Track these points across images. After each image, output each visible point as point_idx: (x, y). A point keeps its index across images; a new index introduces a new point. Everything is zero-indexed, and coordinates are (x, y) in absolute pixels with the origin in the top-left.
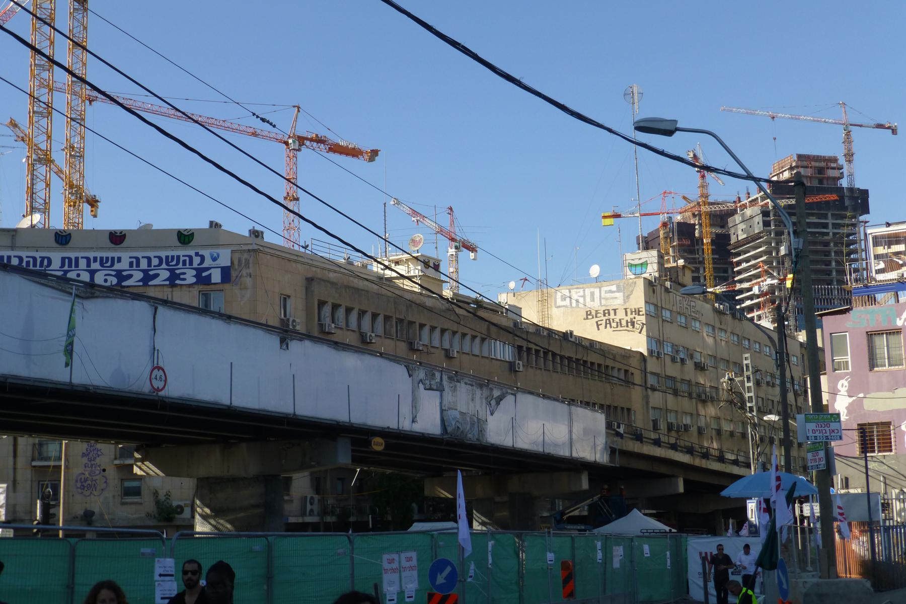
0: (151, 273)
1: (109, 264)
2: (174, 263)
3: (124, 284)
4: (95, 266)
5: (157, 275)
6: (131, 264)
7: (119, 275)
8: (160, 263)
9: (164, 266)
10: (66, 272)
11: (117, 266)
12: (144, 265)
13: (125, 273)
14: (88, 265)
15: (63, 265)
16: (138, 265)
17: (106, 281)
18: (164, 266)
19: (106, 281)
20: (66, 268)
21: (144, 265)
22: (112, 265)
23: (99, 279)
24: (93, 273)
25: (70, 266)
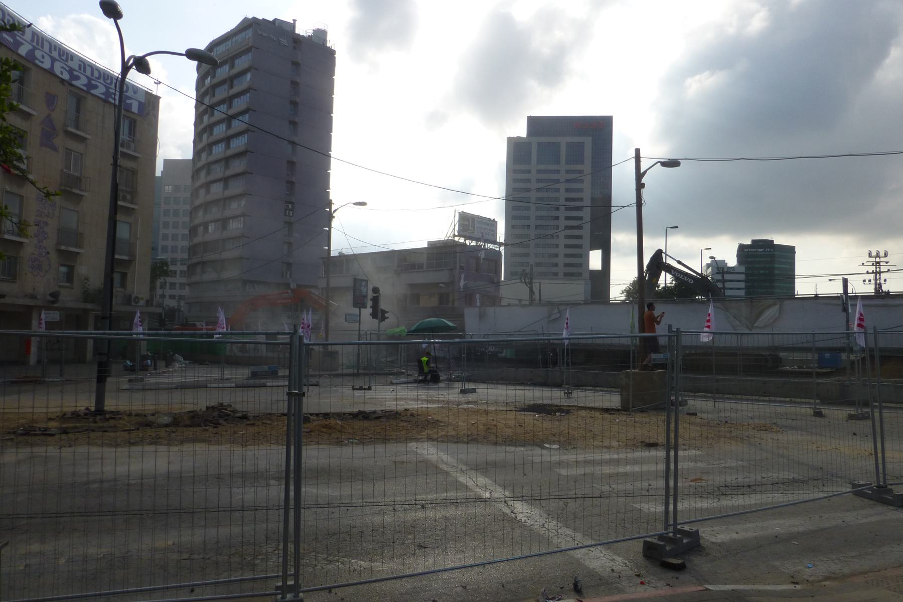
0: (93, 82)
1: (64, 58)
2: (109, 81)
3: (74, 82)
4: (55, 54)
5: (96, 87)
6: (80, 66)
7: (71, 71)
8: (99, 78)
9: (101, 81)
10: (35, 48)
11: (70, 63)
12: (88, 73)
13: (75, 73)
14: (50, 51)
15: (32, 41)
16: (85, 71)
17: (62, 73)
18: (101, 81)
19: (62, 73)
20: (35, 44)
21: (88, 73)
22: (67, 60)
23: (57, 70)
24: (53, 60)
25: (38, 44)
